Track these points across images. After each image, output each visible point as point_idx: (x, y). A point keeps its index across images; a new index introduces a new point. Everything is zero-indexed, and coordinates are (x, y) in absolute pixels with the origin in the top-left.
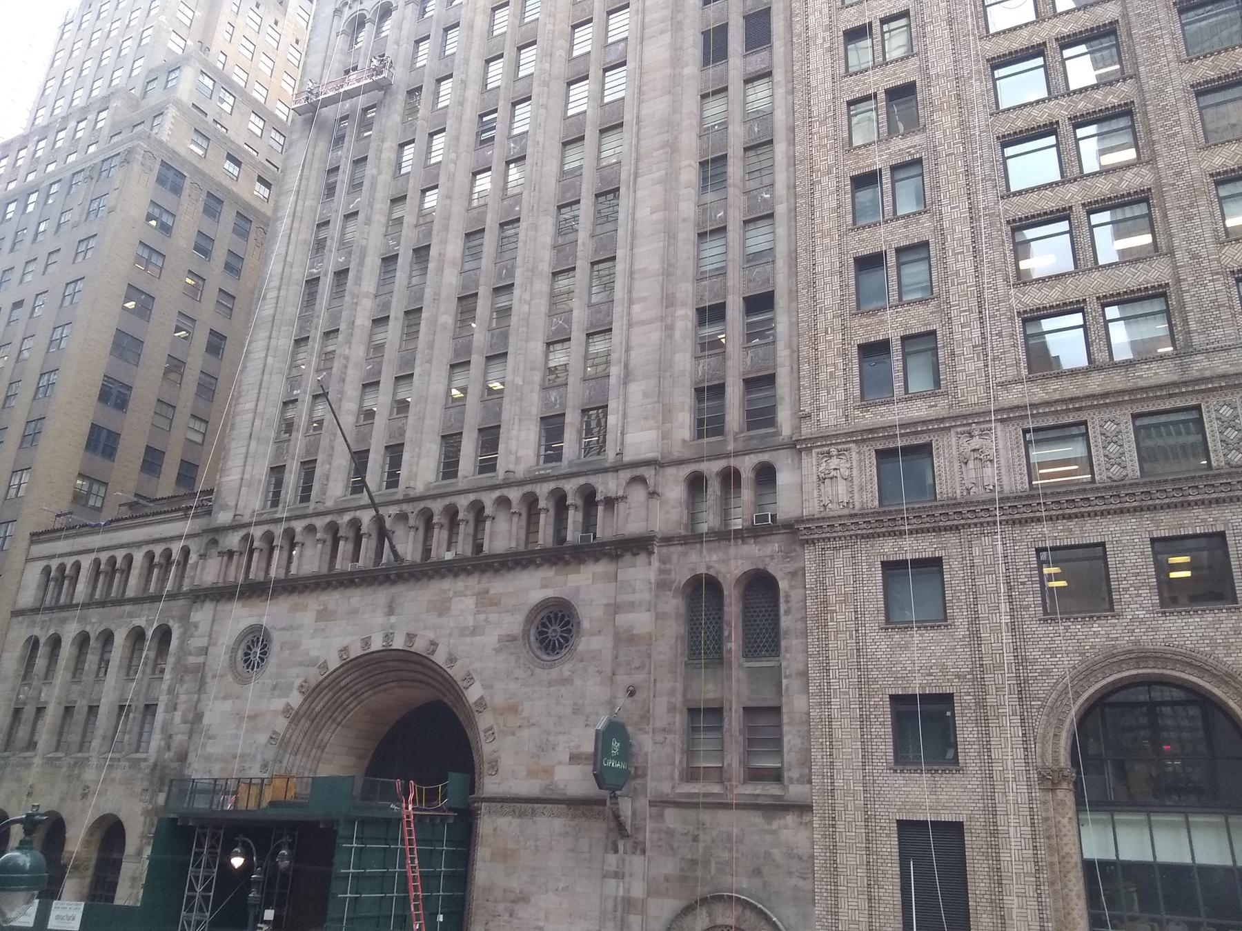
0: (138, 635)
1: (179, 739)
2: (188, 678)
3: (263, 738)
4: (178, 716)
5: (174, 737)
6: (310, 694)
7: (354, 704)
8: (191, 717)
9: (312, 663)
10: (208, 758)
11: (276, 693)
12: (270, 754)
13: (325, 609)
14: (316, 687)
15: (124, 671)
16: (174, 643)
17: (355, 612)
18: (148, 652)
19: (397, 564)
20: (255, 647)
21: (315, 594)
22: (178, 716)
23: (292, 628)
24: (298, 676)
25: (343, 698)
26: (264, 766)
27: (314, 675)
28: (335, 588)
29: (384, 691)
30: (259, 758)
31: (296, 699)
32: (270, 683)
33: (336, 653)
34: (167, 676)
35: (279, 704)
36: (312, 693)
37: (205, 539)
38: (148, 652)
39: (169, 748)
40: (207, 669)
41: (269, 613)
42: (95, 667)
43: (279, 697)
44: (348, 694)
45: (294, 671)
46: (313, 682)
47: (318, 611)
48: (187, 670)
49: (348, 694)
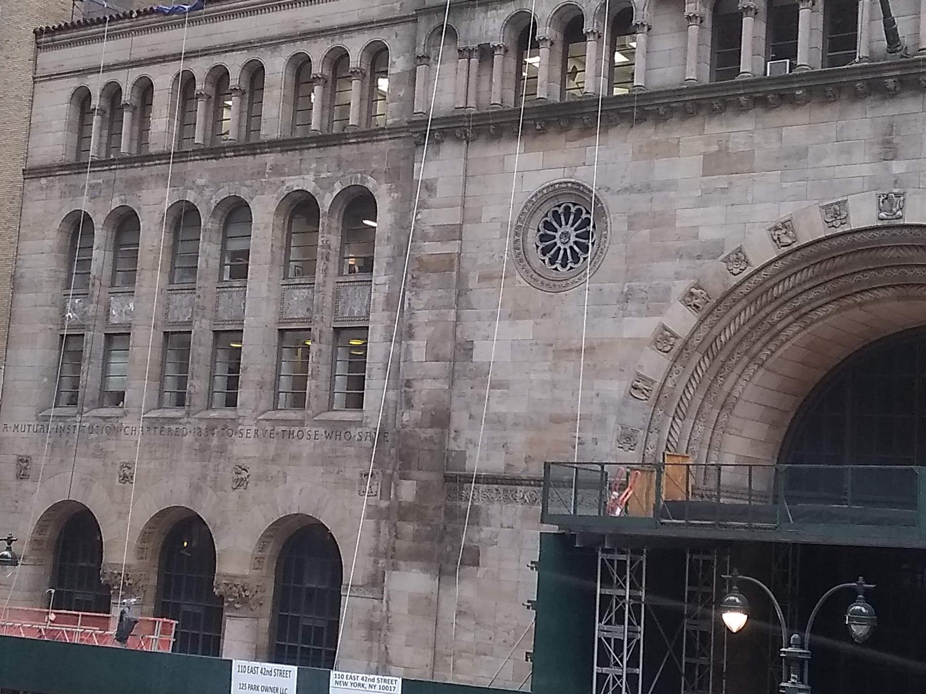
0: (301, 208)
1: (428, 388)
2: (427, 280)
3: (616, 388)
4: (418, 349)
5: (417, 385)
6: (710, 313)
7: (795, 328)
8: (447, 349)
9: (712, 251)
10: (497, 422)
11: (631, 307)
12: (637, 417)
13: (723, 151)
14: (719, 302)
15: (278, 271)
16: (383, 222)
17: (801, 154)
18: (329, 235)
19: (896, 58)
20: (566, 227)
21: (690, 124)
22: (418, 349)
23: (648, 188)
24: (678, 276)
25: (775, 318)
26: (627, 438)
27: (717, 277)
28: (741, 109)
29: (860, 305)
30: (612, 422)
31: (681, 320)
32: (613, 288)
33: (766, 235)
34: (380, 276)
35: (644, 327)
36: (710, 307)
37: (424, 26)
38: (329, 235)
39: (409, 404)
40: (466, 264)
41: (599, 162)
42: (215, 263)
43: (640, 314)
44: (786, 310)
45: (669, 267)
46: (718, 290)
47: (707, 156)
48: (423, 266)
49: (786, 310)
